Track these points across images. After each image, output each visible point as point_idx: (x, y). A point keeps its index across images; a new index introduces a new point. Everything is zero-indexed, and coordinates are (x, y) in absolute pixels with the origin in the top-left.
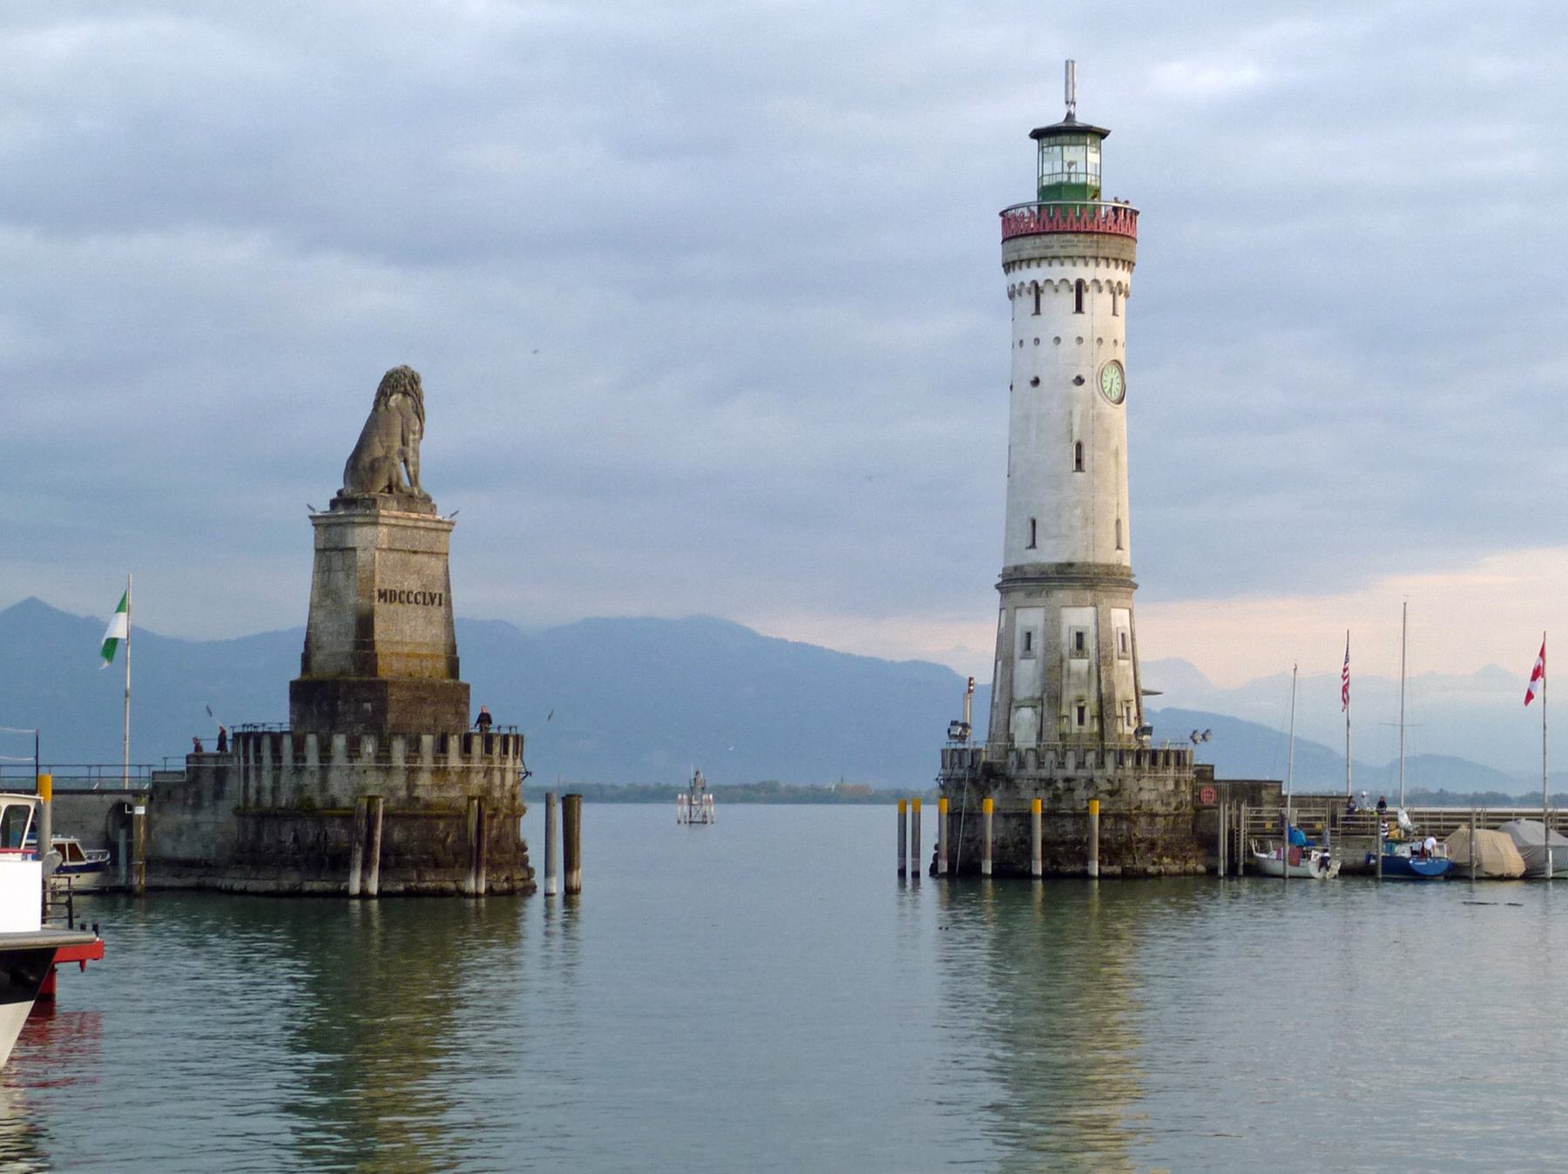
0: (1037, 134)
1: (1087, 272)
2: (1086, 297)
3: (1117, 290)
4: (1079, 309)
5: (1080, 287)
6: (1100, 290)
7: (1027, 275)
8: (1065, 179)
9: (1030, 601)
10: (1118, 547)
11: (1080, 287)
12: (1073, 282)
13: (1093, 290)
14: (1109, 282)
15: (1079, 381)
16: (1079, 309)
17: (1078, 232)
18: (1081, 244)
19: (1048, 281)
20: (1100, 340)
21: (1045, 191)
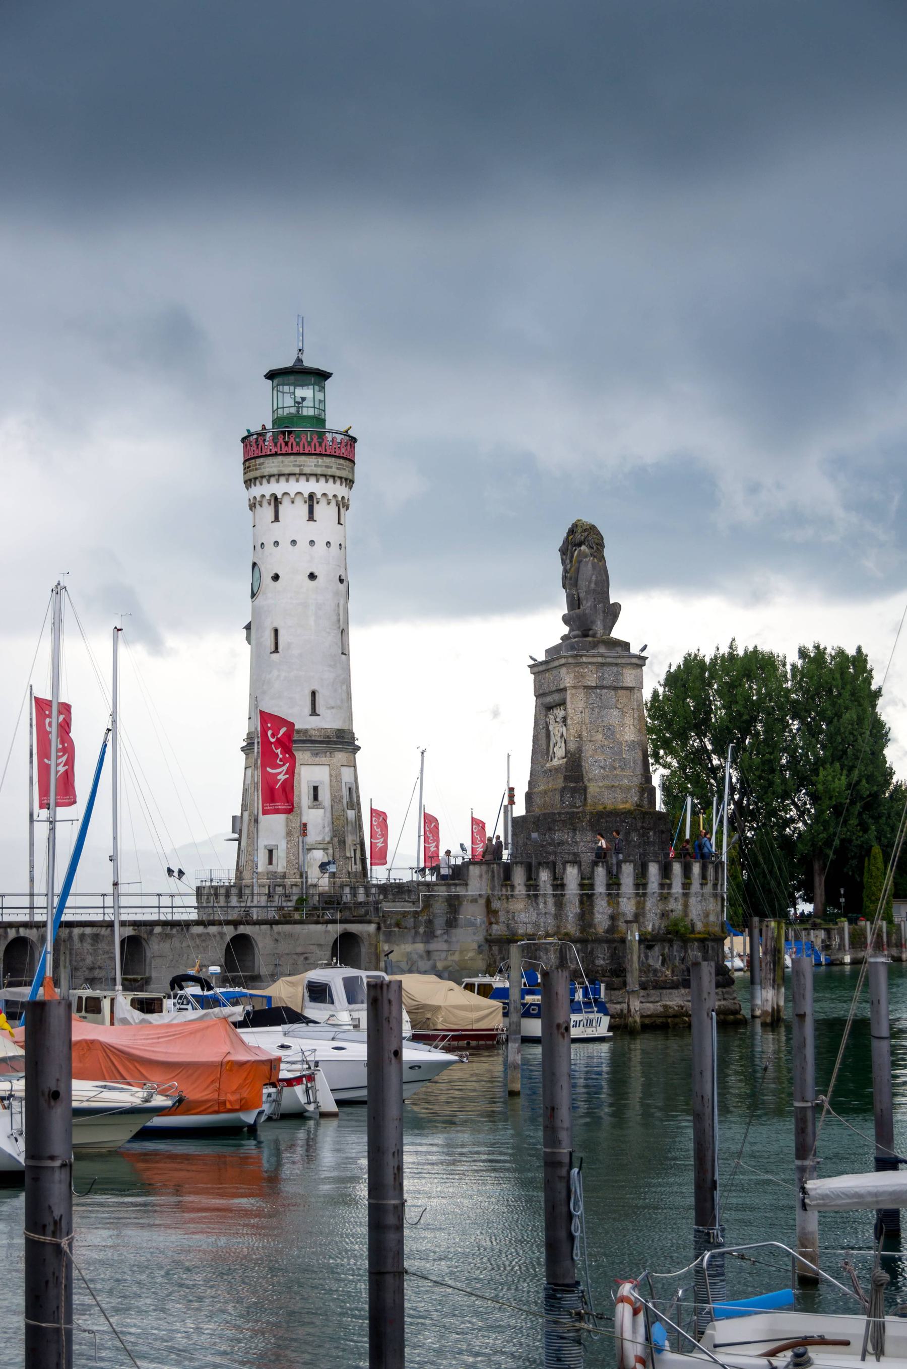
0: (271, 375)
1: (278, 488)
2: (281, 507)
4: (277, 519)
5: (276, 501)
6: (293, 502)
7: (258, 490)
8: (293, 410)
9: (317, 760)
10: (314, 712)
11: (276, 501)
12: (268, 497)
13: (286, 502)
14: (299, 493)
15: (276, 578)
16: (277, 519)
17: (310, 454)
18: (311, 464)
19: (263, 496)
21: (274, 422)
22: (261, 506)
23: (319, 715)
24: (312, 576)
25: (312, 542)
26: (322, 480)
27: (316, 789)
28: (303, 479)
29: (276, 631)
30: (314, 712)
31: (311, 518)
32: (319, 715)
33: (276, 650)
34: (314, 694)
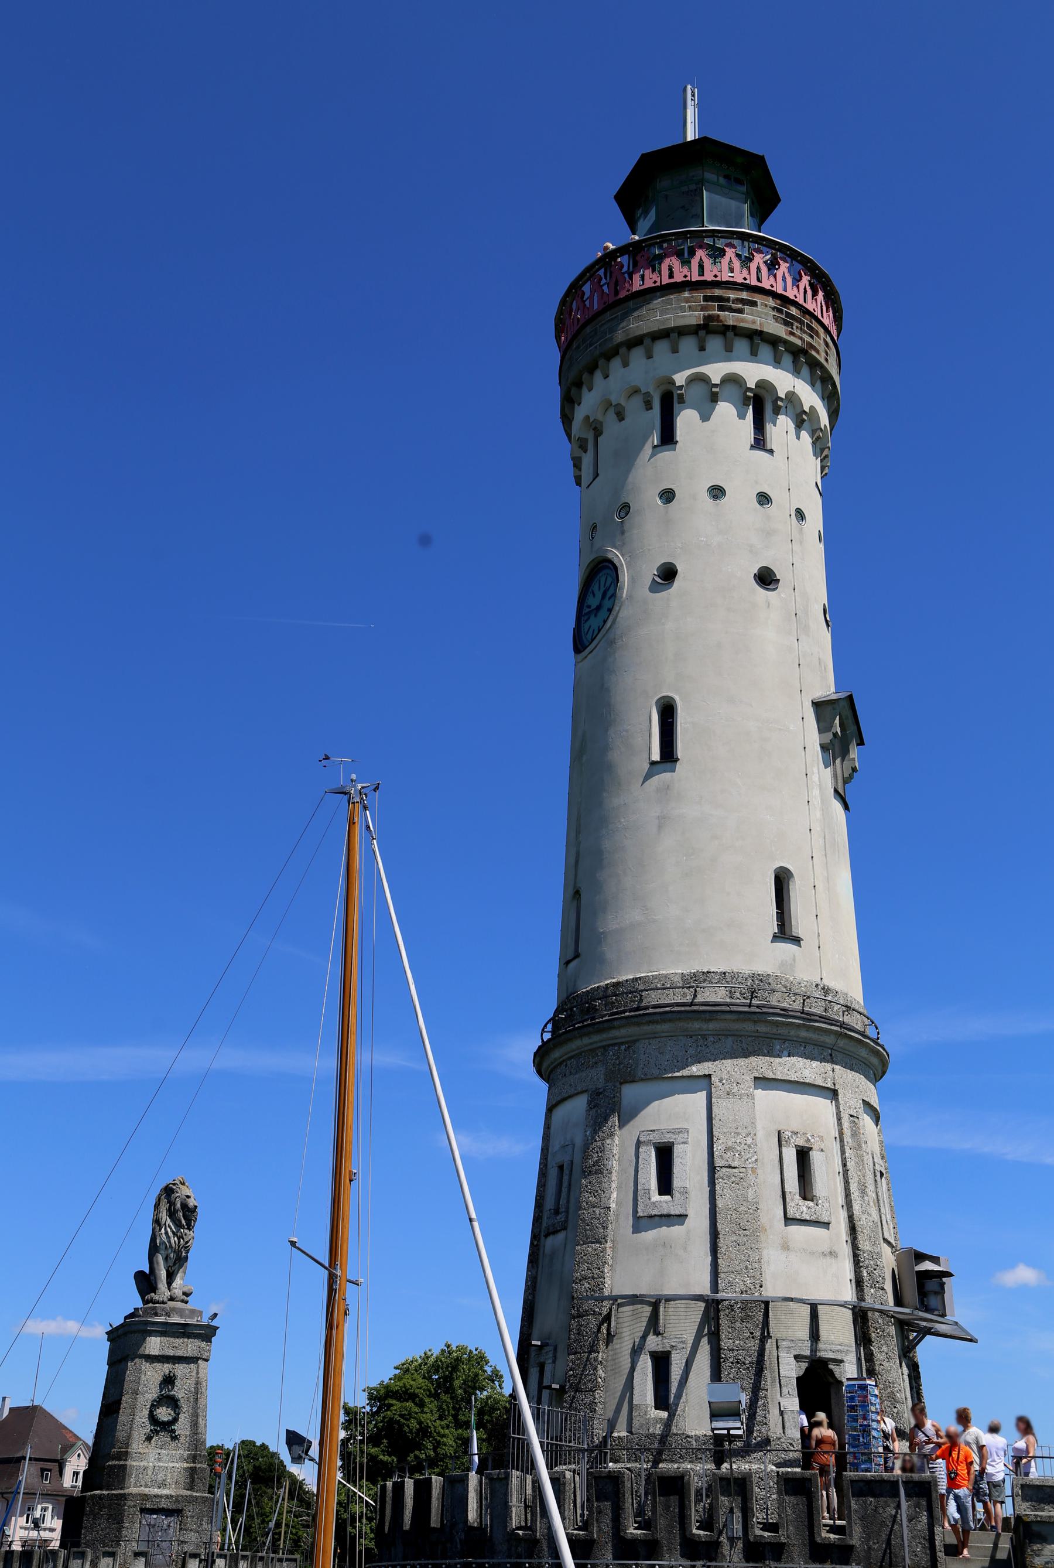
3: (760, 404)
4: (668, 438)
10: (784, 932)
15: (668, 574)
20: (717, 492)
22: (620, 416)
23: (797, 941)
24: (766, 578)
25: (764, 499)
26: (787, 359)
27: (803, 1156)
28: (741, 345)
29: (667, 711)
30: (784, 932)
31: (760, 443)
32: (797, 941)
33: (669, 754)
34: (782, 881)
